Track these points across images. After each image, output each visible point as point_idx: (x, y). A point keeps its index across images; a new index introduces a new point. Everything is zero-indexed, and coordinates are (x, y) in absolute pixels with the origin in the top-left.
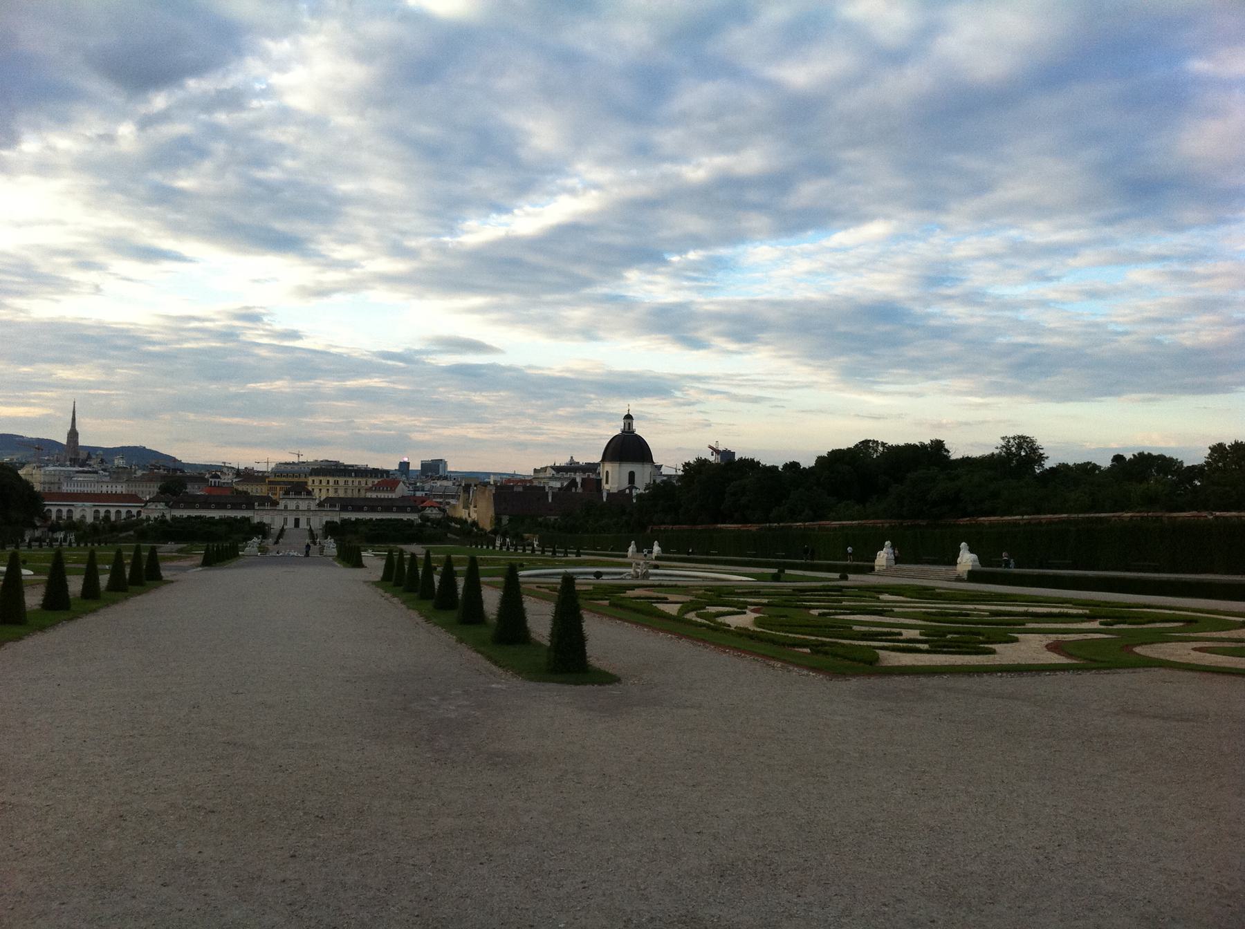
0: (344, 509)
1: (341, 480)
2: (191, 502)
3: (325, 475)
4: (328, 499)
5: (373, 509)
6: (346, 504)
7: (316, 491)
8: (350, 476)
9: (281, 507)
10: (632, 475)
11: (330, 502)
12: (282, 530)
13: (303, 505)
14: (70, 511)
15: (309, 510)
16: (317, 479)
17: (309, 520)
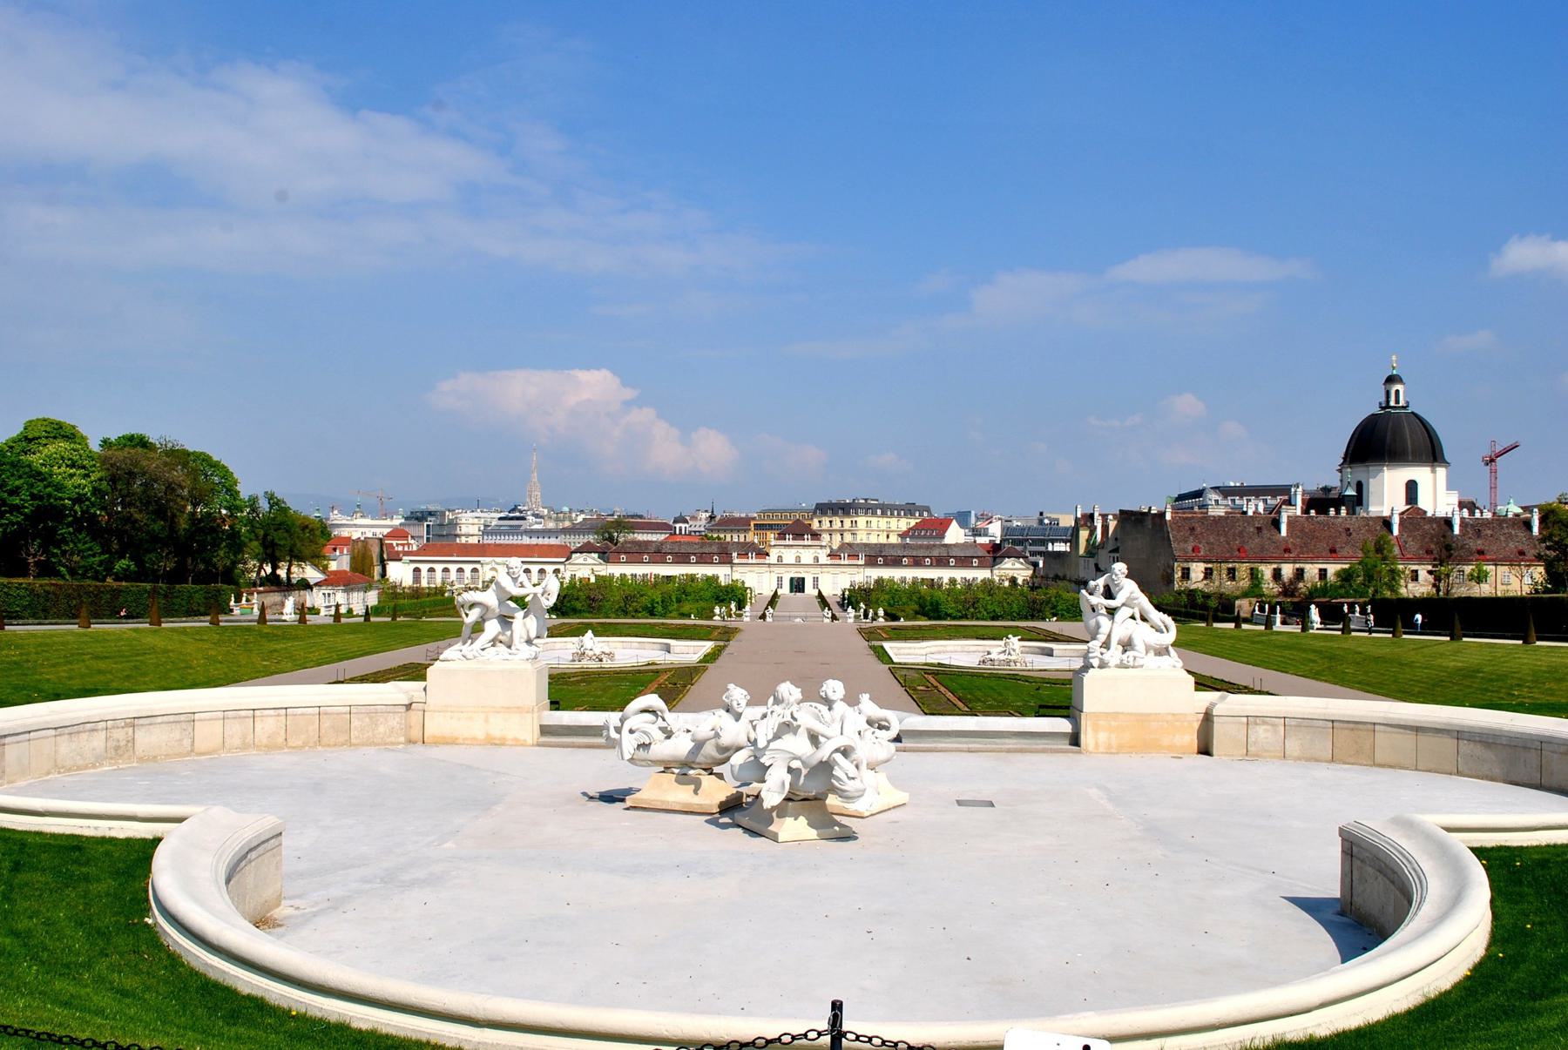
0: (871, 562)
1: (862, 521)
2: (636, 553)
3: (835, 514)
4: (844, 546)
5: (917, 563)
6: (876, 555)
7: (826, 537)
8: (874, 514)
9: (772, 559)
10: (1412, 487)
11: (850, 551)
12: (775, 595)
13: (807, 556)
14: (475, 570)
16: (825, 521)
17: (816, 580)
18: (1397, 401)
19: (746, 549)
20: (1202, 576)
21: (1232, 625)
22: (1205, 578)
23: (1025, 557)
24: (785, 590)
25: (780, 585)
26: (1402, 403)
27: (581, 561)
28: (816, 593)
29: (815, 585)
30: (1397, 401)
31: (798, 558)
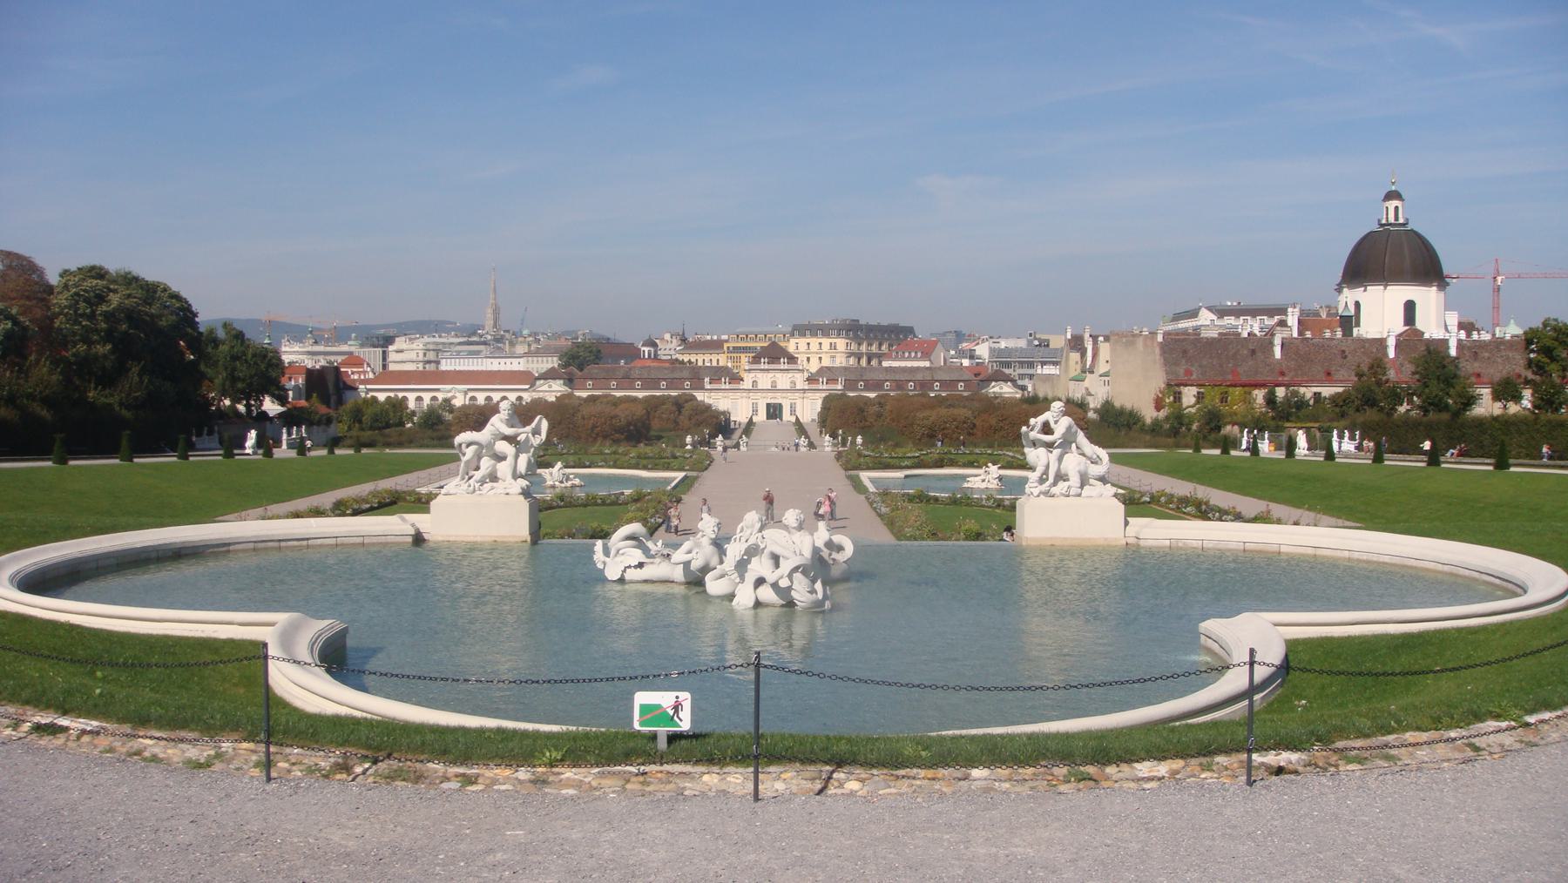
7: (802, 358)
9: (747, 384)
10: (1410, 307)
12: (751, 423)
13: (783, 381)
15: (793, 390)
18: (1396, 218)
19: (718, 374)
20: (1193, 400)
21: (1217, 452)
22: (1198, 402)
23: (1013, 381)
24: (761, 416)
25: (755, 411)
26: (1401, 221)
27: (545, 388)
28: (793, 419)
29: (793, 412)
30: (1396, 218)
31: (774, 384)
